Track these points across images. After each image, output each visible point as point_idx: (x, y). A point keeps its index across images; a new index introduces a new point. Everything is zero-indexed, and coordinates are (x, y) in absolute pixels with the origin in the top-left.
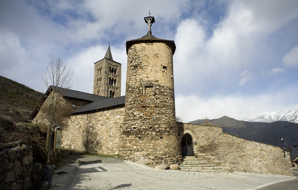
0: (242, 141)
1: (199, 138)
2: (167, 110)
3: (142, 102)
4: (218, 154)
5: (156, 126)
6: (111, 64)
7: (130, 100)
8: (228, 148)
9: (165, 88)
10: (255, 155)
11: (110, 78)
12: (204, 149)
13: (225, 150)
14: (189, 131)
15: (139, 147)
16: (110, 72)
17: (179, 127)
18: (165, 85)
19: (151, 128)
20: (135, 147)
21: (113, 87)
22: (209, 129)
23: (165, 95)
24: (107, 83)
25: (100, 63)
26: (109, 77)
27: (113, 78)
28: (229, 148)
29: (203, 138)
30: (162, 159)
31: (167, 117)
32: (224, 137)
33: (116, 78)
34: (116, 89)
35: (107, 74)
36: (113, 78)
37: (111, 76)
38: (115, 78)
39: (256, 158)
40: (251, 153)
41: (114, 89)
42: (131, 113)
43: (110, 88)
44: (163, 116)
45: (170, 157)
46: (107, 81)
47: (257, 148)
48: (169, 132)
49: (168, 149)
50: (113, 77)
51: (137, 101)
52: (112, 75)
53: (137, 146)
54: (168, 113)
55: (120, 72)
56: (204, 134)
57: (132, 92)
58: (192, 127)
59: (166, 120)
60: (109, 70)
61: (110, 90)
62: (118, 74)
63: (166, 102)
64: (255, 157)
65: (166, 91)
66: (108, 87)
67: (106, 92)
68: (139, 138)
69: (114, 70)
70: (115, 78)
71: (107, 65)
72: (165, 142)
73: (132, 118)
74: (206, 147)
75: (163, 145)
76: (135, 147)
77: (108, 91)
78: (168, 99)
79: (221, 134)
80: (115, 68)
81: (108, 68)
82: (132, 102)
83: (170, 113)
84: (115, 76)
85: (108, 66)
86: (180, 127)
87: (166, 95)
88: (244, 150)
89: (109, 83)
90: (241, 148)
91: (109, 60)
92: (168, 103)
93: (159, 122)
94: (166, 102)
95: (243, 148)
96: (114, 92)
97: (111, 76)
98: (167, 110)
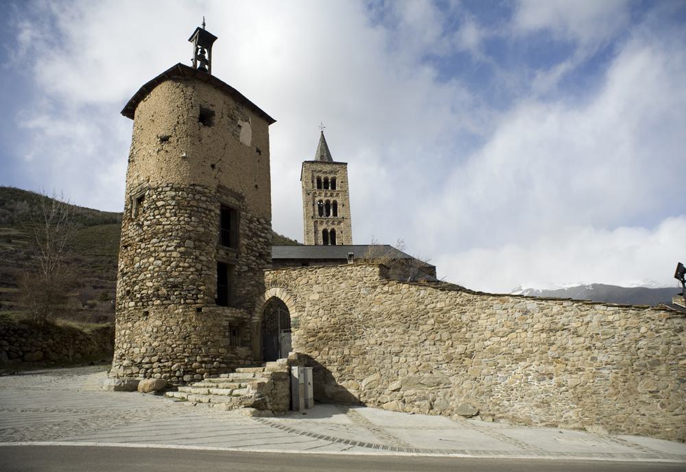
0: (459, 300)
1: (304, 307)
2: (161, 244)
4: (365, 353)
6: (320, 171)
8: (400, 330)
9: (160, 190)
10: (519, 351)
11: (321, 201)
12: (321, 339)
13: (388, 339)
14: (278, 289)
16: (319, 187)
17: (253, 282)
18: (160, 183)
21: (328, 221)
22: (334, 276)
23: (157, 208)
24: (312, 214)
26: (317, 199)
27: (328, 202)
28: (405, 332)
29: (317, 307)
31: (160, 259)
32: (384, 296)
33: (334, 199)
34: (336, 223)
35: (311, 196)
36: (328, 202)
37: (322, 198)
38: (332, 199)
39: (522, 364)
40: (499, 343)
41: (333, 224)
43: (322, 223)
44: (152, 259)
45: (162, 361)
46: (312, 209)
47: (529, 321)
49: (161, 341)
50: (327, 198)
52: (323, 194)
54: (164, 251)
55: (345, 181)
56: (319, 293)
58: (287, 276)
59: (157, 269)
60: (316, 185)
61: (321, 229)
62: (341, 188)
63: (159, 223)
64: (518, 360)
65: (162, 196)
66: (316, 222)
67: (312, 235)
69: (323, 181)
70: (332, 199)
71: (310, 176)
72: (153, 322)
74: (326, 332)
75: (147, 333)
77: (316, 232)
78: (168, 215)
79: (374, 287)
80: (330, 177)
81: (312, 182)
83: (172, 248)
84: (332, 195)
85: (313, 177)
86: (257, 282)
87: (163, 206)
88: (467, 336)
89: (317, 213)
90: (452, 329)
91: (321, 162)
92: (164, 225)
93: (142, 277)
94: (159, 223)
95: (461, 328)
96: (333, 232)
97: (323, 197)
98: (161, 244)
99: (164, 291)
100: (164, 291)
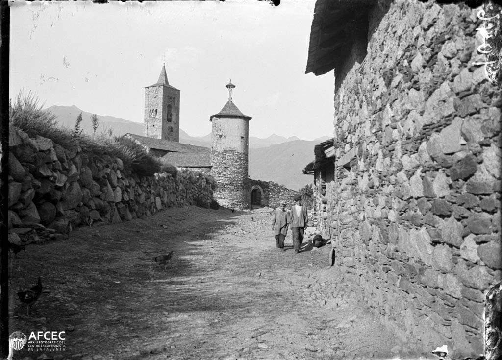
3: (225, 164)
5: (234, 182)
7: (215, 162)
15: (222, 196)
19: (231, 183)
20: (219, 196)
25: (154, 89)
30: (237, 205)
42: (217, 172)
48: (243, 187)
51: (222, 163)
53: (221, 195)
57: (217, 156)
68: (222, 190)
73: (217, 175)
76: (219, 196)
82: (218, 164)
99: (242, 184)
100: (242, 184)
